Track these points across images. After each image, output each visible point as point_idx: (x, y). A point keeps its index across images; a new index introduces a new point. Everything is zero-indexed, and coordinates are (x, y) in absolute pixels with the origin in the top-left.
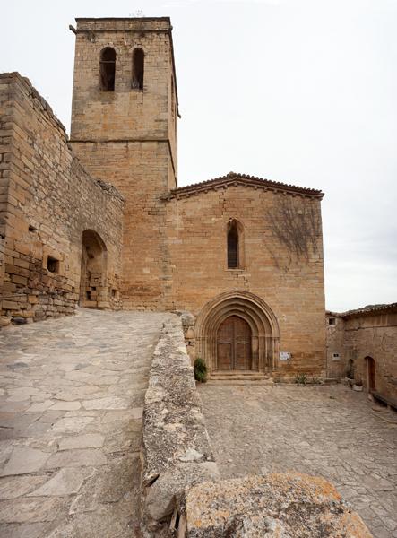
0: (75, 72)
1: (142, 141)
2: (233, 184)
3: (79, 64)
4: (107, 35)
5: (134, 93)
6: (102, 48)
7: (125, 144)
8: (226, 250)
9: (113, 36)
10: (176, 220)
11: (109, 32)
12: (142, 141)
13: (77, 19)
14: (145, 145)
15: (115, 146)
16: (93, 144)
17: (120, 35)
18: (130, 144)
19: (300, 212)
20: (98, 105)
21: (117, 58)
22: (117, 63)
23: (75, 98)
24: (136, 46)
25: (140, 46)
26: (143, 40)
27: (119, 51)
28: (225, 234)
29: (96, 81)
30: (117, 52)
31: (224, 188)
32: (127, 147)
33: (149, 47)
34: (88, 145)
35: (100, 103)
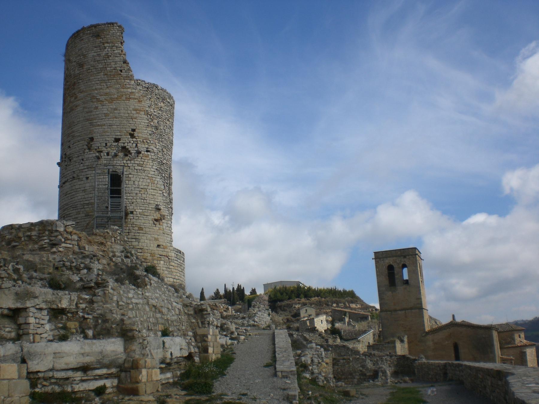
0: (377, 278)
1: (411, 309)
2: (453, 327)
3: (379, 274)
4: (388, 258)
5: (405, 286)
6: (387, 265)
7: (403, 312)
8: (453, 355)
9: (391, 259)
10: (430, 343)
11: (390, 257)
12: (411, 309)
13: (374, 252)
14: (413, 311)
15: (400, 312)
16: (390, 312)
17: (395, 258)
18: (407, 311)
19: (484, 336)
20: (389, 293)
21: (395, 269)
22: (395, 272)
23: (379, 291)
24: (403, 263)
25: (404, 263)
26: (405, 259)
27: (395, 266)
28: (452, 348)
29: (386, 282)
30: (394, 266)
31: (449, 328)
32: (405, 312)
33: (408, 263)
34: (388, 313)
35: (390, 292)
